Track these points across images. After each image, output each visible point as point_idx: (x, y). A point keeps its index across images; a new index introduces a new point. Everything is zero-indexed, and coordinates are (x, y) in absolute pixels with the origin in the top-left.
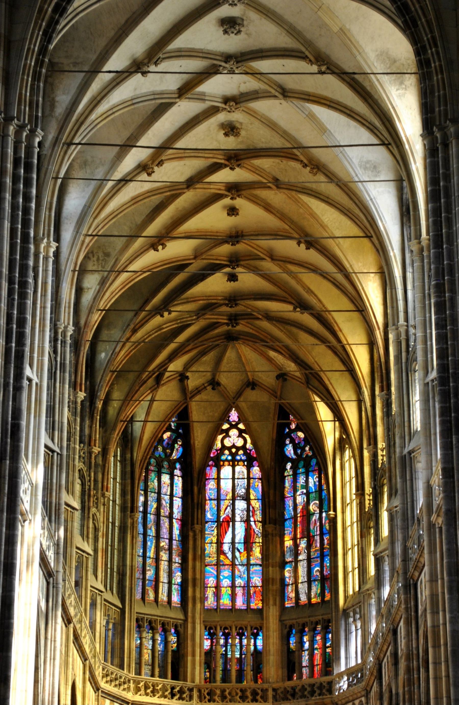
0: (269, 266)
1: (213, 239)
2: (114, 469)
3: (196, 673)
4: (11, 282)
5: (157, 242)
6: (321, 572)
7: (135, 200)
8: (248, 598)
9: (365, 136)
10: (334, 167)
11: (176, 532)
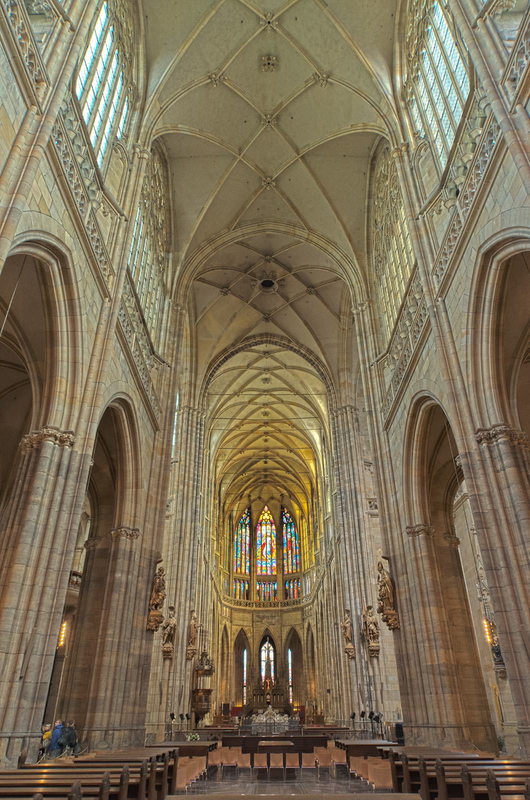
2: (227, 528)
3: (254, 598)
7: (235, 437)
8: (272, 571)
9: (309, 415)
11: (247, 549)
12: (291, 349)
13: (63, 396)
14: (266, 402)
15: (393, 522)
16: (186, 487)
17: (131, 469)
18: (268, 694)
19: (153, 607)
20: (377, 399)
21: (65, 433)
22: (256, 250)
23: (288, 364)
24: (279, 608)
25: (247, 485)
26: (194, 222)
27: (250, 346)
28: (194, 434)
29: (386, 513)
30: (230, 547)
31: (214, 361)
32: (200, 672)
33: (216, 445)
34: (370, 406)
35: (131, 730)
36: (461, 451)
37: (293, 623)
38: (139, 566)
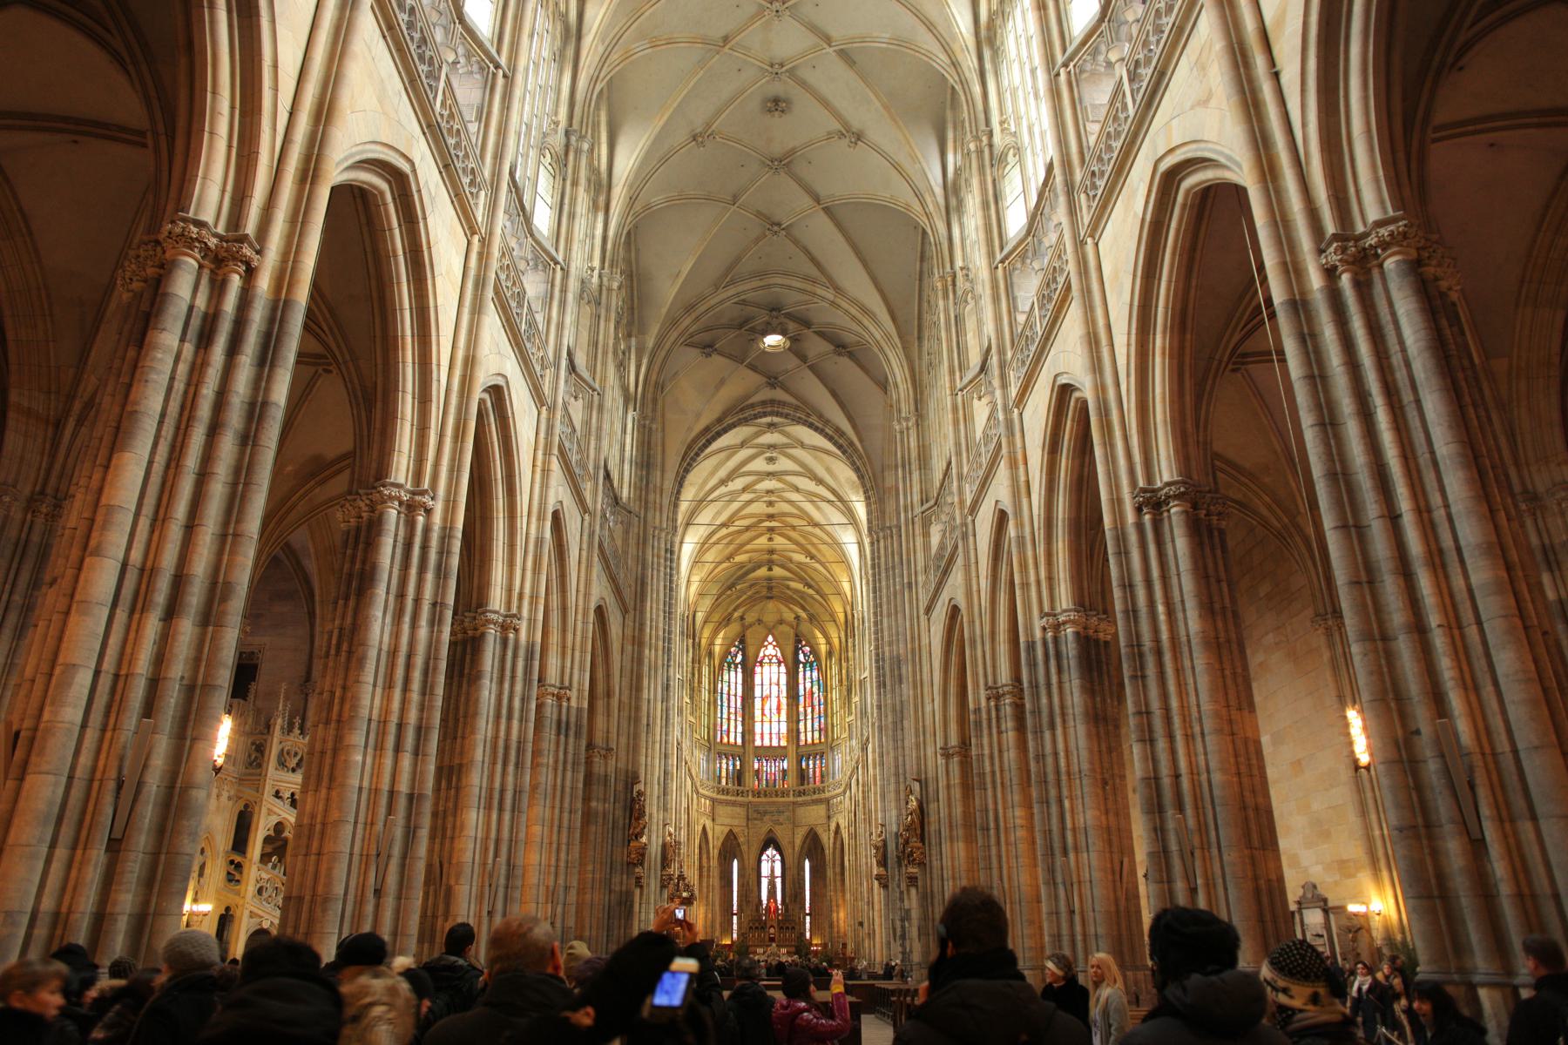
2: (705, 670)
12: (811, 426)
22: (758, 306)
23: (807, 441)
24: (791, 799)
26: (667, 292)
31: (690, 447)
36: (971, 706)
37: (812, 822)
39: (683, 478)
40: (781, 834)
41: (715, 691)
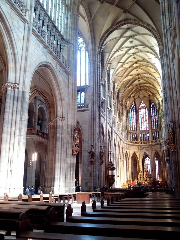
0: (144, 78)
1: (135, 75)
2: (125, 111)
4: (98, 86)
5: (126, 77)
6: (157, 124)
7: (121, 71)
10: (151, 62)
12: (140, 25)
13: (12, 69)
14: (134, 52)
15: (175, 105)
16: (94, 97)
17: (58, 93)
18: (146, 177)
19: (74, 146)
20: (169, 48)
21: (14, 84)
23: (140, 32)
24: (150, 144)
25: (132, 92)
27: (120, 26)
28: (96, 73)
29: (172, 102)
30: (126, 120)
31: (103, 36)
32: (109, 169)
33: (112, 76)
34: (166, 51)
35: (70, 188)
38: (67, 131)
39: (102, 46)
40: (149, 153)
41: (128, 117)
